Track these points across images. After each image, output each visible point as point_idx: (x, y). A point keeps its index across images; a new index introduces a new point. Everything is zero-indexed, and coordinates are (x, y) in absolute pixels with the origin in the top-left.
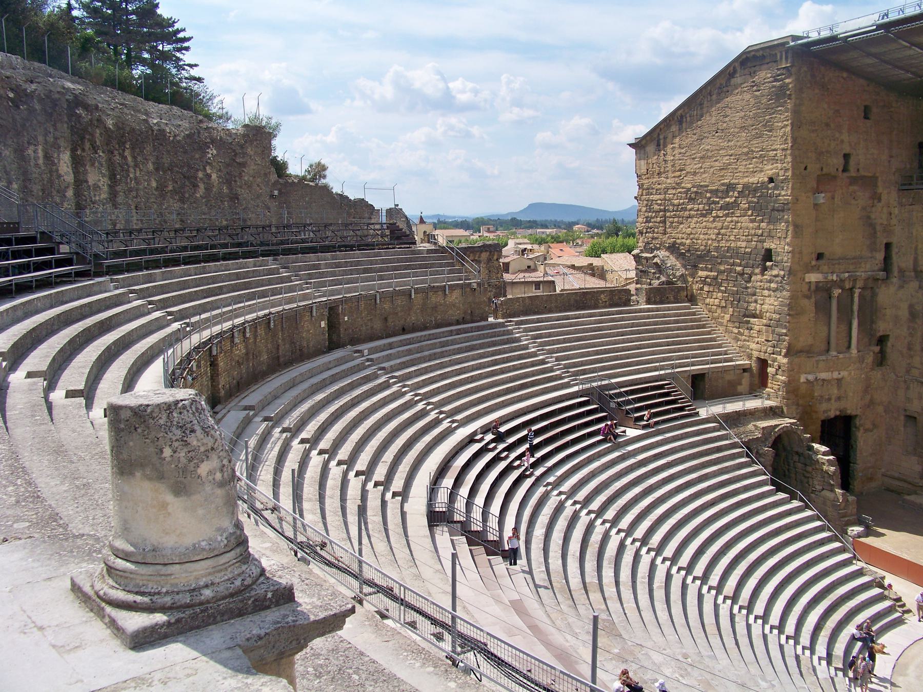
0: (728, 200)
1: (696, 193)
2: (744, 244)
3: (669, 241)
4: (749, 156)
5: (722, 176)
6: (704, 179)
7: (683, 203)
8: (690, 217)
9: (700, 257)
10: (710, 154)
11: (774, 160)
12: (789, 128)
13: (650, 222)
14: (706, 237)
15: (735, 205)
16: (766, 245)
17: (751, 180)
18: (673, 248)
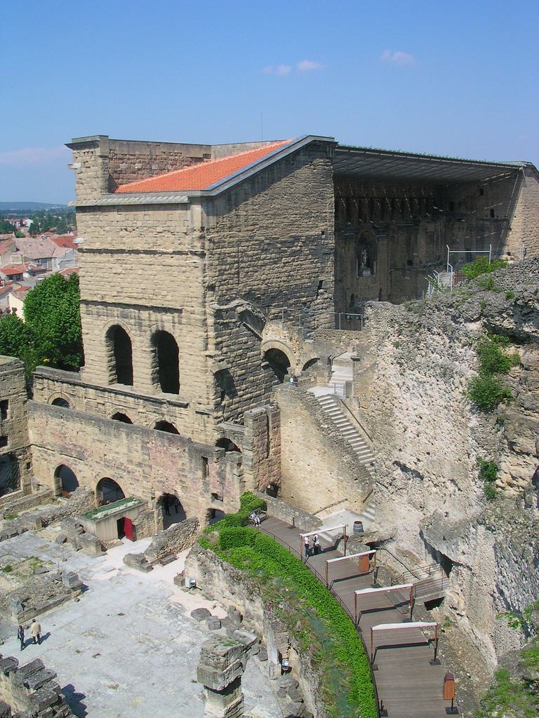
0: (294, 248)
1: (268, 244)
2: (307, 280)
3: (245, 289)
4: (308, 215)
5: (290, 230)
6: (276, 232)
7: (257, 254)
8: (265, 265)
9: (273, 298)
10: (280, 212)
11: (324, 219)
12: (333, 199)
13: (223, 274)
14: (279, 280)
15: (300, 251)
16: (320, 278)
17: (310, 233)
18: (248, 296)
